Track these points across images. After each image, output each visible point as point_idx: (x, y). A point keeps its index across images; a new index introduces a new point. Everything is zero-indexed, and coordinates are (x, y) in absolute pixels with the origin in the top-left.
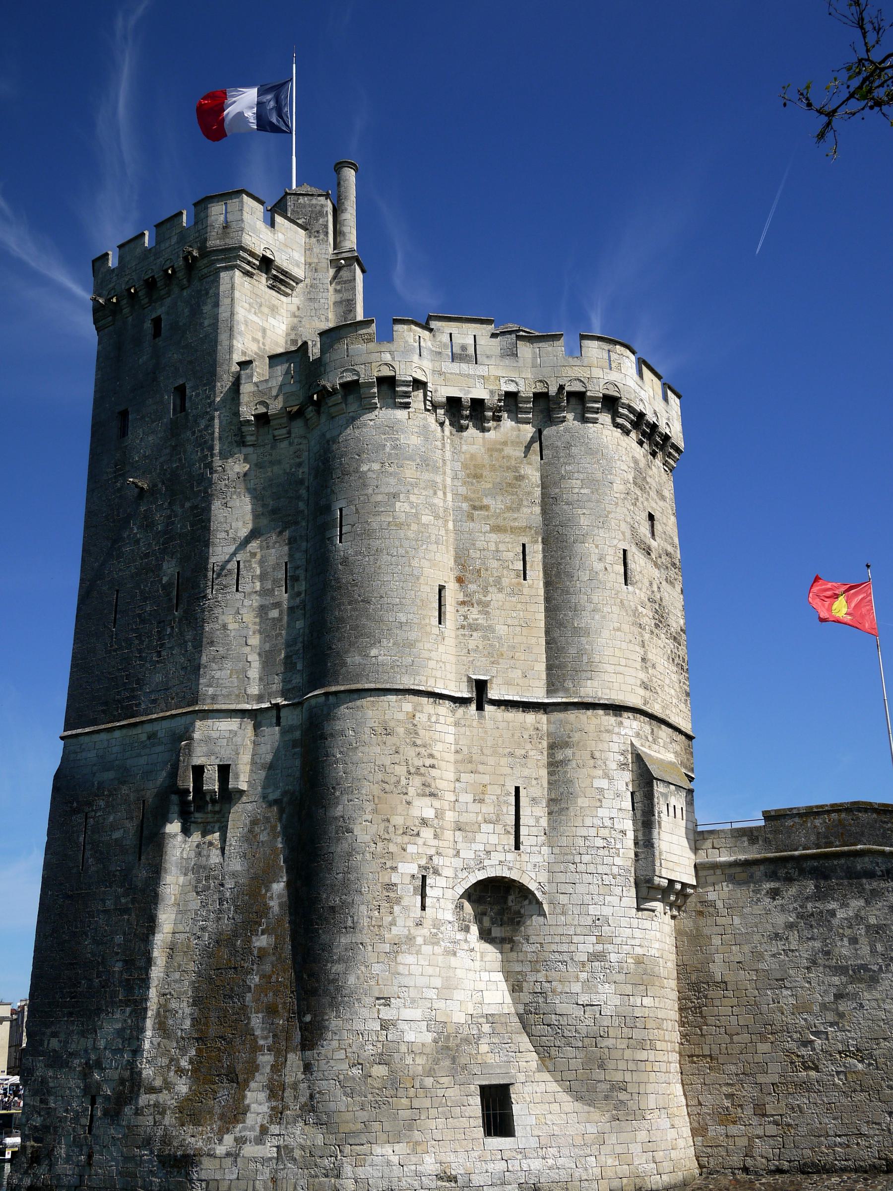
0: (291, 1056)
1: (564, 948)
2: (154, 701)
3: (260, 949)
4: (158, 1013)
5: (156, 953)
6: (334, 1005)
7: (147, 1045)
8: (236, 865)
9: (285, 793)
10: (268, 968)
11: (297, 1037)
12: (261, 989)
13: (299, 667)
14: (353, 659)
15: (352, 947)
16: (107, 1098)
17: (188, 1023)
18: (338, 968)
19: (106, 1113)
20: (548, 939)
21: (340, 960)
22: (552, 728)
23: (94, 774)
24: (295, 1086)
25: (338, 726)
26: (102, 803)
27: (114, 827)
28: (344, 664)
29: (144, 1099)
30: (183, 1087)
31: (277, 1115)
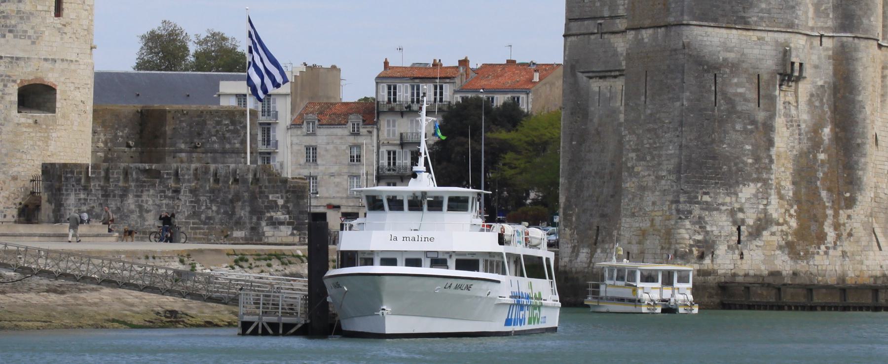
0: (841, 212)
1: (882, 167)
2: (762, 18)
3: (822, 160)
4: (776, 188)
5: (774, 157)
6: (860, 190)
7: (773, 202)
8: (805, 116)
9: (825, 82)
10: (826, 169)
11: (843, 204)
12: (824, 180)
13: (831, 16)
14: (865, 21)
15: (866, 164)
16: (748, 226)
17: (791, 194)
18: (860, 173)
19: (750, 234)
20: (878, 163)
21: (861, 170)
22: (883, 58)
23: (719, 52)
24: (844, 224)
25: (860, 55)
26: (728, 71)
27: (737, 85)
28: (862, 23)
29: (774, 228)
30: (793, 223)
31: (839, 237)
